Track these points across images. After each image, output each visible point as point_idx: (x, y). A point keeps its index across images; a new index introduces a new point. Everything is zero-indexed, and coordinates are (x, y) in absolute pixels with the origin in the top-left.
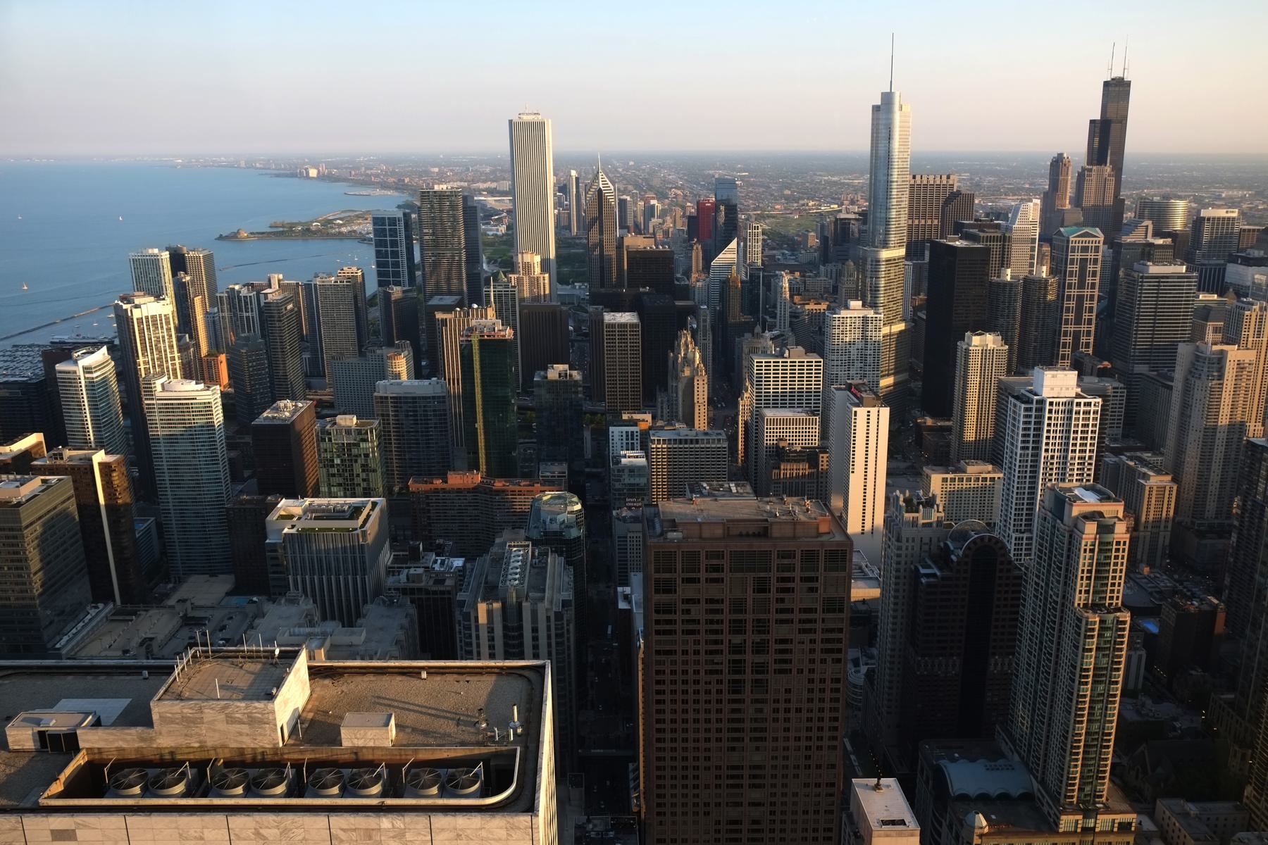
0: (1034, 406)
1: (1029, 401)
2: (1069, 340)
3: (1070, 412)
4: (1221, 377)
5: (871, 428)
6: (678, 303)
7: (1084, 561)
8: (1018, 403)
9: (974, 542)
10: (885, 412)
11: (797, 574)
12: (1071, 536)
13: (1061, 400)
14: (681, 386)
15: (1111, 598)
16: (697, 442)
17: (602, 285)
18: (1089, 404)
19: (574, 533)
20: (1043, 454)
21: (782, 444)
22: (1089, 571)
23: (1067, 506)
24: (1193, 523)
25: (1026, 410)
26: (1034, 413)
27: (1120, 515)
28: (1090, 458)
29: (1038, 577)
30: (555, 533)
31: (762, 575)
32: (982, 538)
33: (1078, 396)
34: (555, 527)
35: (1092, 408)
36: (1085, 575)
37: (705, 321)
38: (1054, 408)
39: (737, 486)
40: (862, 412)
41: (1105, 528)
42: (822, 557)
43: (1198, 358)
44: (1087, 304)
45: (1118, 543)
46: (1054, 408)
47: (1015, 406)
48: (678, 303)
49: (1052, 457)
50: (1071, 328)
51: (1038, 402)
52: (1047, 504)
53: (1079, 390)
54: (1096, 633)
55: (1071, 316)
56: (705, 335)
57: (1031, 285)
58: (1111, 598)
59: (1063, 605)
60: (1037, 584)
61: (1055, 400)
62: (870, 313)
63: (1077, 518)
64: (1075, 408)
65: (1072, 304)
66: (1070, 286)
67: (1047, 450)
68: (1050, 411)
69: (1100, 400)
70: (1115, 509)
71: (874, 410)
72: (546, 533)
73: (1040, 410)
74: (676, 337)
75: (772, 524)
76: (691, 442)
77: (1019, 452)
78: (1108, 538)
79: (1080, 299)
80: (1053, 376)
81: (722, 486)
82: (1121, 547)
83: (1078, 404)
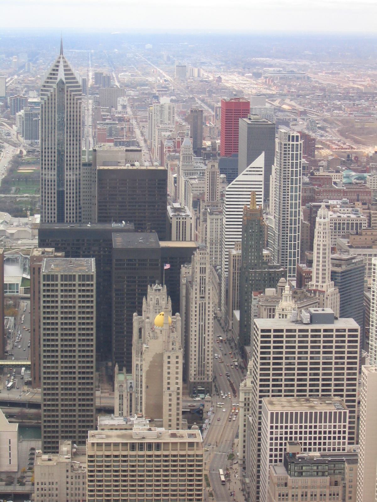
6: (163, 244)
14: (145, 368)
16: (158, 446)
17: (61, 219)
21: (290, 449)
37: (203, 270)
48: (163, 244)
56: (202, 291)
76: (150, 446)
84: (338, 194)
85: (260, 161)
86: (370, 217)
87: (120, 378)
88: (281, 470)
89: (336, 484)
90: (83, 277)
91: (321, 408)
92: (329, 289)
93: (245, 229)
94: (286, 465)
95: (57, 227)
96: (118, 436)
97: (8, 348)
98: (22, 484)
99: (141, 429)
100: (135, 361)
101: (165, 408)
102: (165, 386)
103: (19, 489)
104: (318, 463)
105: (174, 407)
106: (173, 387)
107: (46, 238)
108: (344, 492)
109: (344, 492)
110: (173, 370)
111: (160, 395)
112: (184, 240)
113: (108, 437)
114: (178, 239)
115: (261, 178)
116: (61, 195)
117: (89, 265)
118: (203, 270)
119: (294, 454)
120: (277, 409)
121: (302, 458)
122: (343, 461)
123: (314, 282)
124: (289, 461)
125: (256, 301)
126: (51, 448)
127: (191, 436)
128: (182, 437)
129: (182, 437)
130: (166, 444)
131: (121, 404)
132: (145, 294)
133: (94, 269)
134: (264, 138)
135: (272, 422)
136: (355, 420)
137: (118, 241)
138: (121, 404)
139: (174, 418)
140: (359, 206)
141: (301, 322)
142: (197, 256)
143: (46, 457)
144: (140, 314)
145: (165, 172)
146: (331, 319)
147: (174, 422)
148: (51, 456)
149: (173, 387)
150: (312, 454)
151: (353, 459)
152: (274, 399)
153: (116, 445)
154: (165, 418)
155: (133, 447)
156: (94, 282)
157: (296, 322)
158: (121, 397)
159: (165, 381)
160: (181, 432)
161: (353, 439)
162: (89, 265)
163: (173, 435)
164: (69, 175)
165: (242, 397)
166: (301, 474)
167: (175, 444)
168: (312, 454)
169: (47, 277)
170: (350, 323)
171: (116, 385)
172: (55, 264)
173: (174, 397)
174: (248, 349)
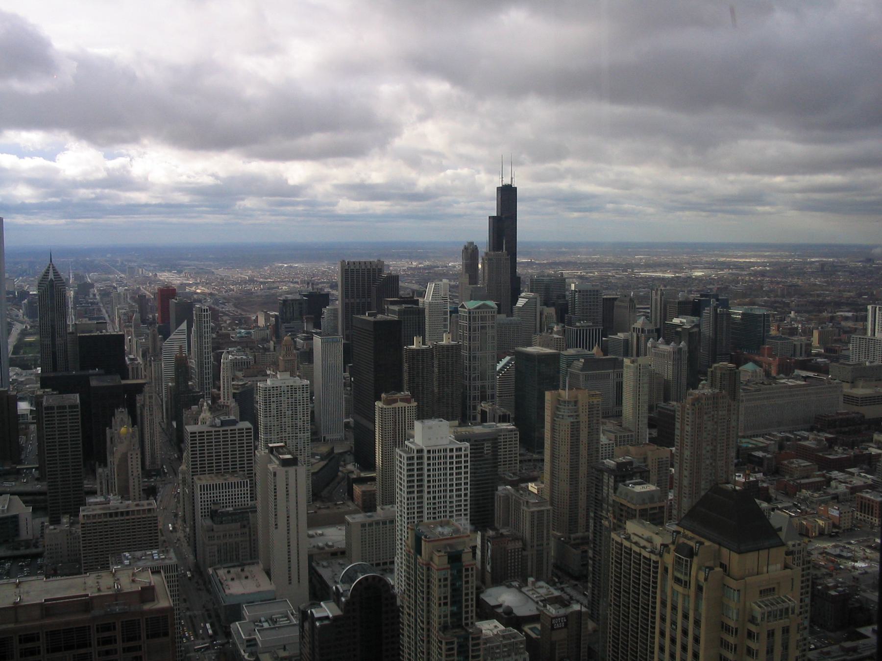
2: (478, 393)
6: (124, 382)
11: (119, 645)
12: (428, 569)
13: (437, 448)
16: (128, 513)
17: (55, 369)
18: (460, 449)
20: (426, 495)
24: (570, 538)
26: (415, 461)
28: (466, 495)
31: (82, 651)
32: (366, 578)
33: (451, 442)
35: (463, 453)
37: (151, 397)
38: (431, 455)
40: (281, 471)
41: (455, 558)
43: (559, 402)
46: (431, 455)
47: (401, 456)
48: (124, 382)
49: (434, 498)
50: (478, 383)
51: (418, 451)
52: (409, 542)
53: (452, 437)
54: (455, 652)
59: (428, 630)
60: (409, 615)
61: (431, 449)
67: (429, 493)
68: (429, 458)
69: (468, 444)
71: (291, 470)
73: (421, 458)
75: (92, 598)
76: (122, 513)
77: (405, 495)
82: (470, 573)
83: (451, 450)
84: (234, 344)
85: (184, 326)
86: (255, 357)
87: (100, 470)
88: (208, 522)
89: (244, 526)
90: (71, 407)
91: (232, 480)
92: (232, 403)
93: (177, 369)
94: (212, 518)
95: (52, 375)
96: (101, 509)
97: (23, 457)
98: (37, 547)
99: (115, 501)
100: (109, 459)
101: (131, 489)
103: (34, 550)
104: (232, 514)
105: (137, 487)
107: (45, 382)
108: (250, 531)
109: (250, 531)
111: (127, 481)
112: (137, 378)
113: (93, 510)
114: (133, 378)
115: (185, 336)
116: (54, 354)
117: (76, 398)
118: (151, 397)
119: (216, 511)
120: (204, 482)
121: (222, 512)
122: (247, 512)
123: (222, 399)
124: (214, 515)
125: (186, 414)
126: (55, 521)
127: (149, 504)
128: (143, 506)
129: (143, 506)
130: (133, 511)
131: (101, 488)
132: (113, 415)
133: (78, 401)
134: (186, 310)
136: (253, 485)
137: (94, 383)
138: (101, 488)
139: (137, 494)
140: (248, 351)
141: (215, 426)
142: (146, 389)
143: (52, 527)
144: (111, 428)
145: (123, 336)
146: (234, 422)
147: (137, 496)
148: (56, 526)
149: (135, 474)
150: (228, 509)
151: (254, 510)
152: (202, 476)
153: (100, 515)
154: (131, 494)
155: (111, 515)
156: (79, 409)
157: (212, 426)
158: (101, 483)
160: (142, 502)
161: (253, 497)
162: (76, 398)
163: (137, 505)
164: (59, 341)
165: (180, 476)
166: (221, 523)
167: (138, 511)
168: (228, 509)
169: (47, 408)
170: (247, 424)
171: (98, 476)
172: (51, 399)
173: (136, 480)
174: (182, 445)
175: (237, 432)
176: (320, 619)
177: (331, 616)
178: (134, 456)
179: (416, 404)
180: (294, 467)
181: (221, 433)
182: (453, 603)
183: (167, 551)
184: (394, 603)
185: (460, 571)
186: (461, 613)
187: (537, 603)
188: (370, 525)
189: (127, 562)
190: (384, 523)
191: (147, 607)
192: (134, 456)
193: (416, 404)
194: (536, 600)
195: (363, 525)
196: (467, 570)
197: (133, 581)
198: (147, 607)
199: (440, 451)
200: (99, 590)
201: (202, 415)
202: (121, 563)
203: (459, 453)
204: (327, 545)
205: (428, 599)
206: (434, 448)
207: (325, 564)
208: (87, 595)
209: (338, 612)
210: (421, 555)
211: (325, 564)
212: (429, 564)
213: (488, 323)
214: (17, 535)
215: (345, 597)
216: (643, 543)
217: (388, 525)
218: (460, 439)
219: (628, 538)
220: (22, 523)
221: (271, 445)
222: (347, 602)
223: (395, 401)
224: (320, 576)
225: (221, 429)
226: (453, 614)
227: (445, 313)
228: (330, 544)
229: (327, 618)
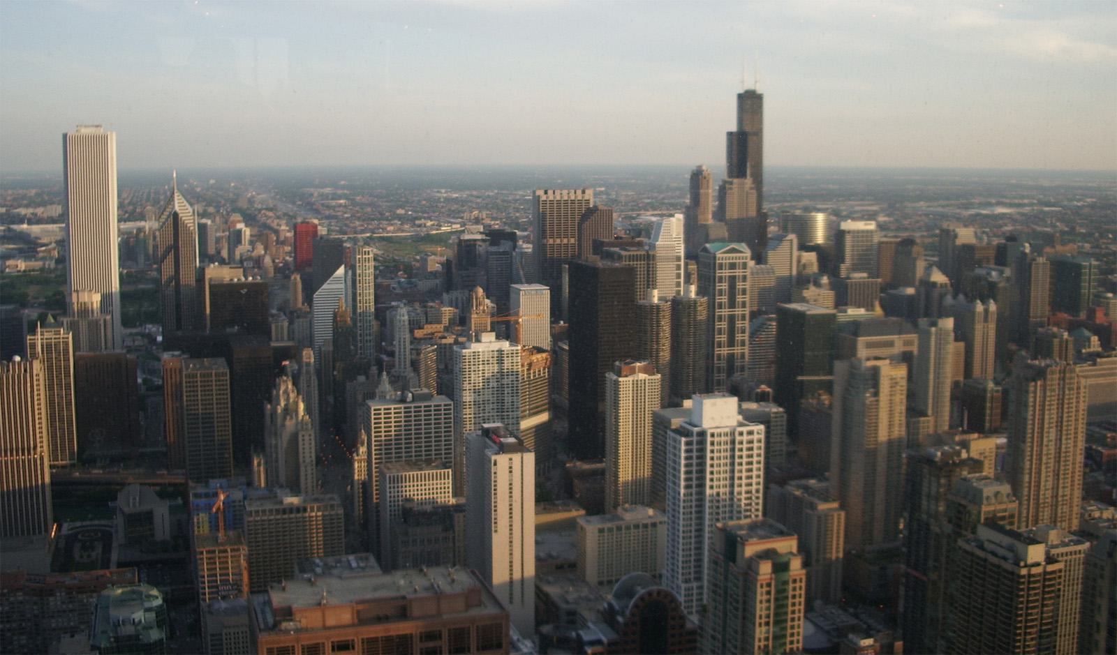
0: (695, 439)
1: (687, 434)
2: (723, 364)
3: (733, 442)
4: (876, 394)
5: (515, 476)
7: (762, 606)
8: (678, 437)
9: (642, 599)
10: (530, 458)
12: (745, 581)
13: (722, 430)
14: (285, 445)
15: (792, 642)
17: (179, 327)
18: (750, 433)
19: (155, 635)
21: (408, 505)
22: (768, 616)
23: (739, 546)
25: (687, 444)
27: (795, 550)
28: (757, 491)
29: (714, 630)
30: (130, 637)
32: (650, 594)
34: (129, 630)
35: (755, 437)
36: (763, 621)
38: (716, 439)
39: (356, 559)
41: (781, 567)
42: (473, 634)
44: (739, 324)
45: (795, 581)
46: (716, 439)
47: (675, 441)
53: (740, 418)
55: (724, 338)
57: (679, 307)
58: (792, 642)
60: (713, 637)
61: (716, 431)
62: (505, 345)
63: (751, 558)
64: (738, 438)
65: (724, 325)
66: (720, 306)
68: (712, 444)
69: (762, 427)
70: (786, 545)
71: (516, 457)
72: (117, 639)
74: (275, 386)
78: (784, 576)
79: (732, 319)
80: (714, 404)
81: (340, 561)
82: (798, 585)
83: (741, 434)
85: (341, 271)
89: (446, 530)
102: (301, 460)
106: (308, 460)
110: (307, 446)
112: (282, 340)
115: (343, 286)
116: (178, 306)
135: (390, 483)
140: (417, 305)
146: (428, 397)
149: (308, 460)
152: (389, 465)
155: (284, 512)
159: (301, 455)
170: (442, 401)
173: (309, 469)
175: (432, 408)
176: (592, 643)
177: (605, 640)
178: (307, 438)
179: (659, 376)
180: (519, 454)
181: (382, 412)
182: (776, 623)
183: (367, 559)
184: (682, 626)
185: (786, 583)
186: (784, 636)
187: (828, 632)
188: (610, 530)
189: (319, 570)
190: (628, 528)
191: (474, 612)
192: (307, 438)
193: (659, 376)
194: (827, 628)
195: (601, 531)
196: (795, 581)
197: (453, 581)
198: (474, 612)
199: (726, 434)
200: (415, 591)
201: (381, 388)
202: (313, 571)
203: (750, 437)
204: (550, 556)
205: (744, 618)
206: (719, 430)
207: (551, 579)
208: (404, 598)
209: (614, 636)
210: (734, 560)
211: (551, 579)
212: (746, 574)
213: (738, 272)
214: (153, 535)
215: (623, 615)
216: (1002, 552)
217: (632, 530)
218: (750, 418)
219: (981, 547)
220: (157, 520)
221: (486, 426)
222: (626, 624)
223: (633, 372)
224: (547, 595)
225: (413, 405)
226: (776, 638)
227: (678, 259)
228: (554, 554)
229: (599, 642)
